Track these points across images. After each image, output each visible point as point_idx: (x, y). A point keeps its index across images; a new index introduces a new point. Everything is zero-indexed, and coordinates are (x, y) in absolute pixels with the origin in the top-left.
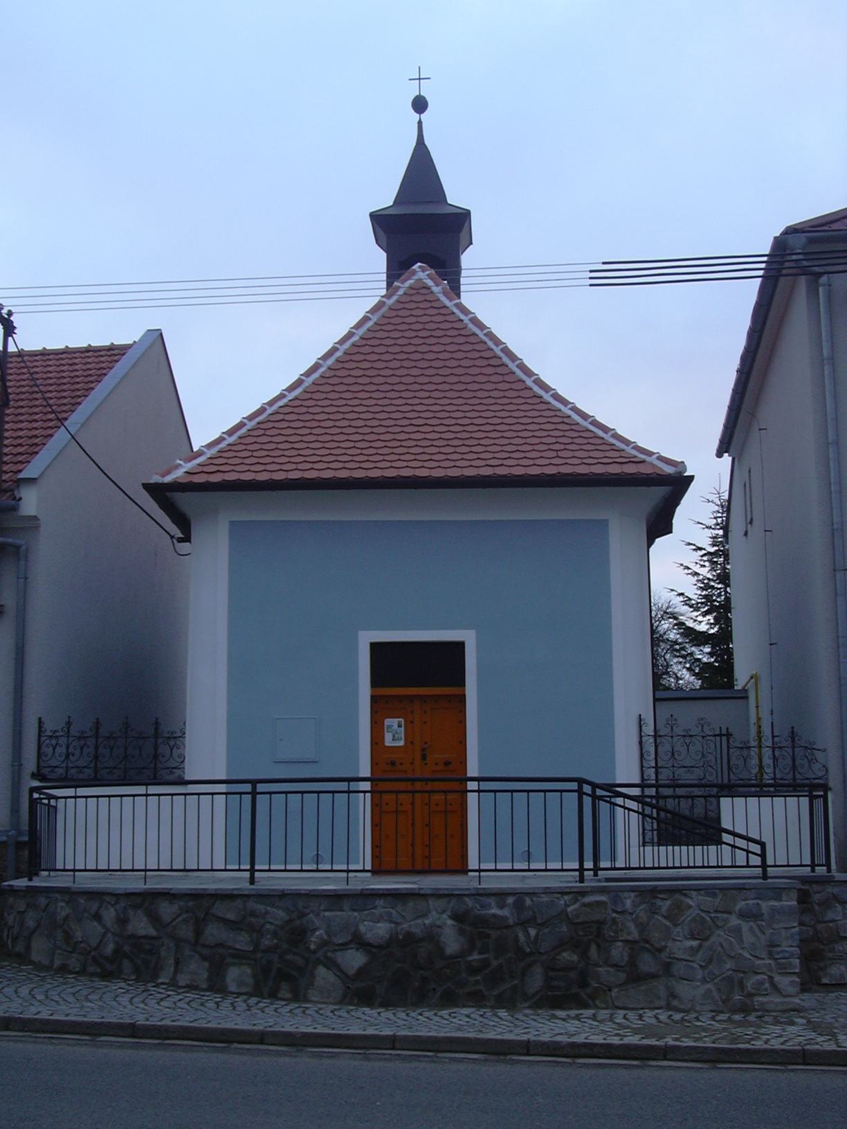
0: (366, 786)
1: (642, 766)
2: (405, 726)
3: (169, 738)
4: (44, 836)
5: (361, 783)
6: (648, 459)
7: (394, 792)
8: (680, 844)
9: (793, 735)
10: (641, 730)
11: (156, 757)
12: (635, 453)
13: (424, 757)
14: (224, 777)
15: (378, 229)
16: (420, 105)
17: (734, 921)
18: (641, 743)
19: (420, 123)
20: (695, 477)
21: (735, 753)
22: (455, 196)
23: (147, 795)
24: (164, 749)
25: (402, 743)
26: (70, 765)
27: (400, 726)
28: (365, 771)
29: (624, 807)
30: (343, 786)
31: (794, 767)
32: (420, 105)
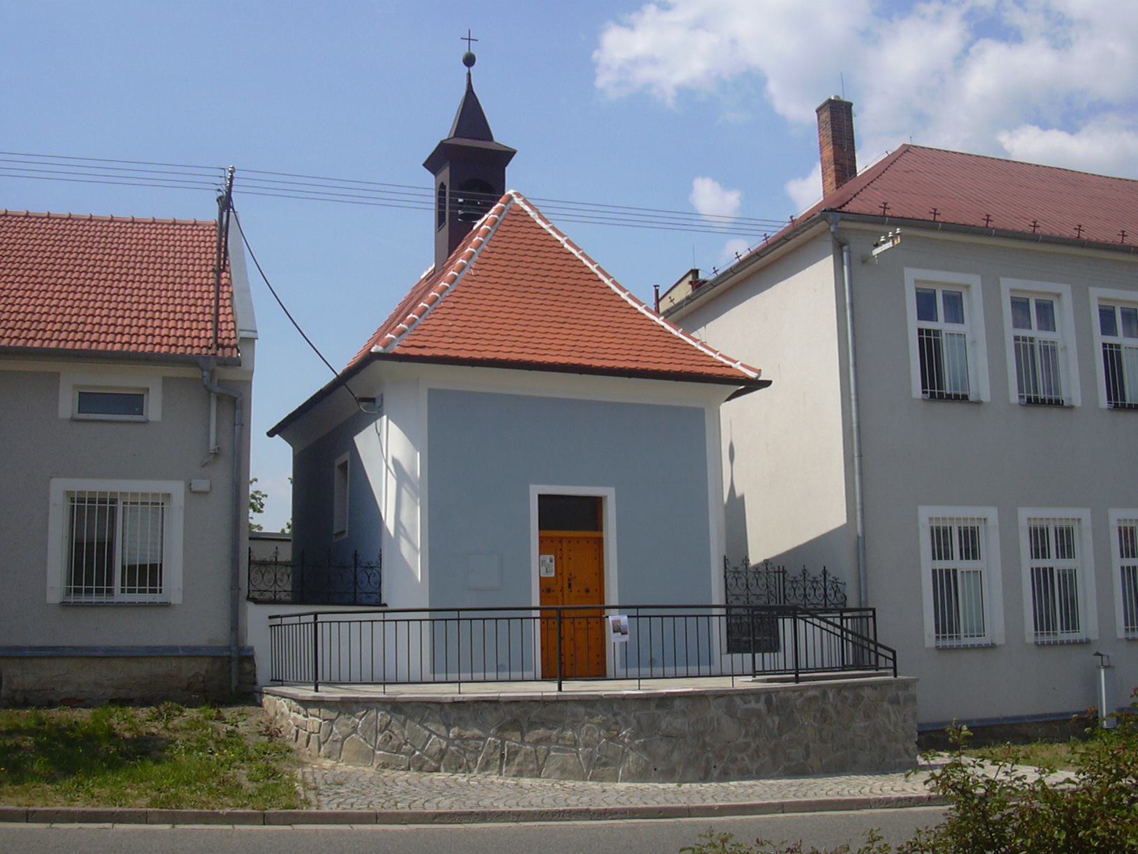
0: (537, 613)
1: (726, 595)
2: (556, 562)
3: (366, 567)
4: (140, 670)
5: (533, 611)
6: (733, 365)
7: (481, 619)
8: (771, 652)
9: (825, 572)
10: (725, 568)
11: (355, 583)
12: (721, 359)
13: (570, 586)
14: (427, 606)
15: (506, 149)
16: (469, 61)
17: (886, 705)
18: (725, 577)
19: (469, 74)
20: (772, 385)
21: (788, 585)
22: (501, 136)
23: (638, 617)
24: (362, 576)
25: (553, 575)
26: (278, 589)
27: (551, 561)
28: (536, 602)
29: (820, 627)
30: (454, 615)
31: (825, 596)
32: (469, 61)
